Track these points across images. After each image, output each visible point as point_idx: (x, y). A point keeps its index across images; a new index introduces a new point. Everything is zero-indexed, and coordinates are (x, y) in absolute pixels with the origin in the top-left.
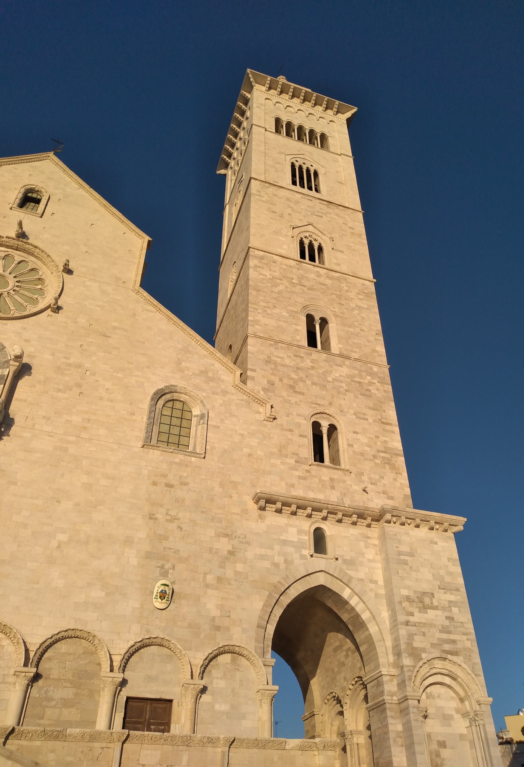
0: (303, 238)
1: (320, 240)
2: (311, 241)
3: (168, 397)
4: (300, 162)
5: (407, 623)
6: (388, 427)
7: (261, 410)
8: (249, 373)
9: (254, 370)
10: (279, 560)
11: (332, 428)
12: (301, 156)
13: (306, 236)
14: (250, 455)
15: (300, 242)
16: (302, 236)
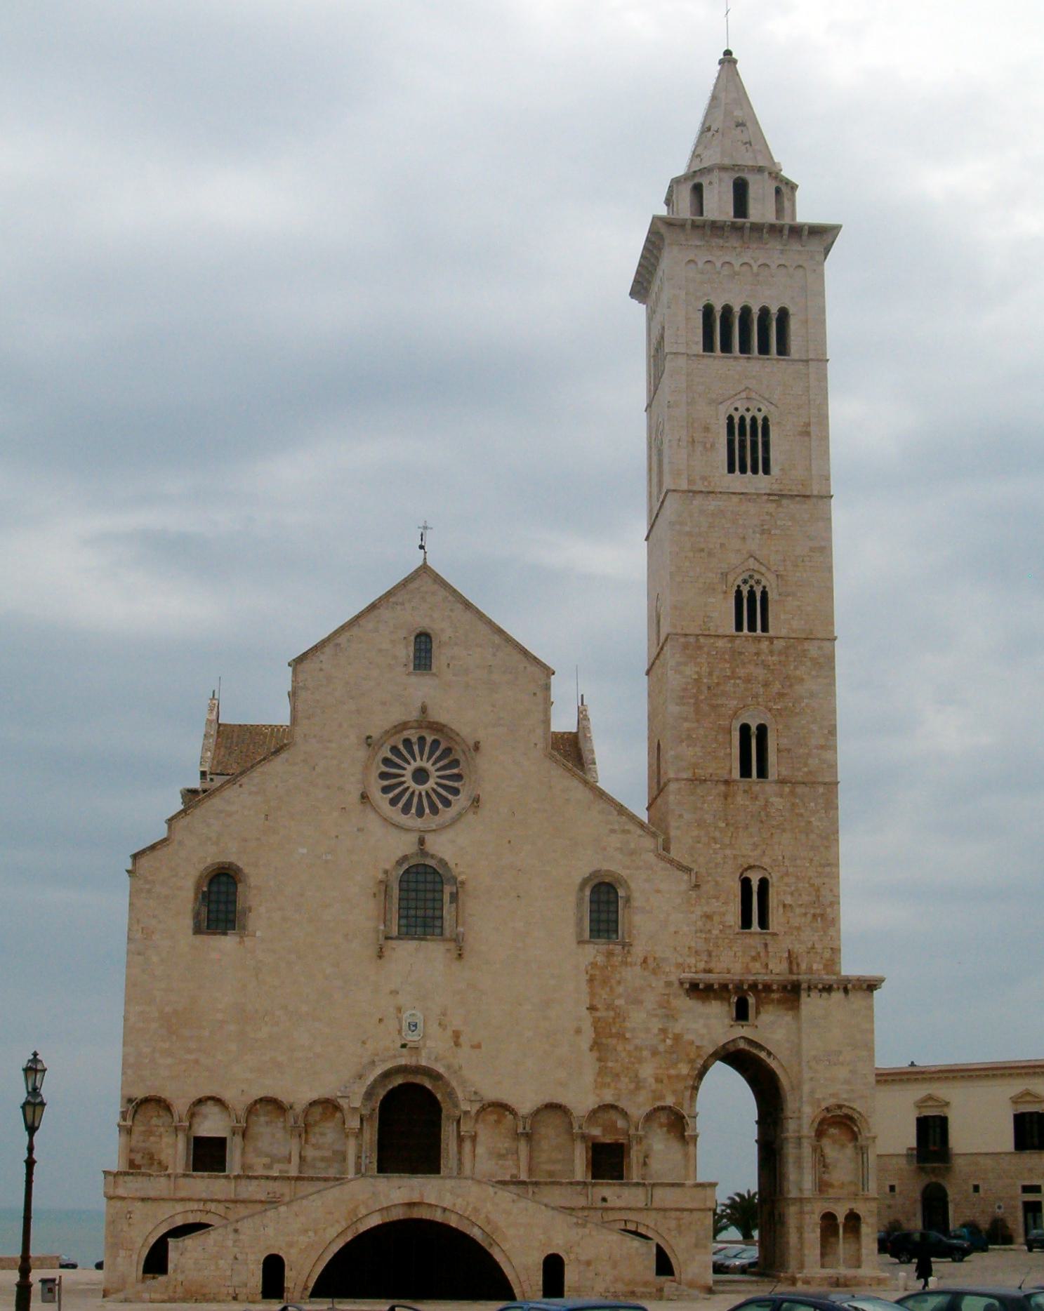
0: (741, 584)
1: (764, 582)
2: (751, 587)
3: (595, 881)
4: (742, 411)
5: (811, 1079)
6: (827, 869)
7: (686, 877)
8: (673, 833)
9: (678, 828)
10: (704, 1031)
11: (764, 884)
12: (744, 395)
13: (745, 580)
14: (675, 933)
15: (735, 597)
16: (739, 582)
